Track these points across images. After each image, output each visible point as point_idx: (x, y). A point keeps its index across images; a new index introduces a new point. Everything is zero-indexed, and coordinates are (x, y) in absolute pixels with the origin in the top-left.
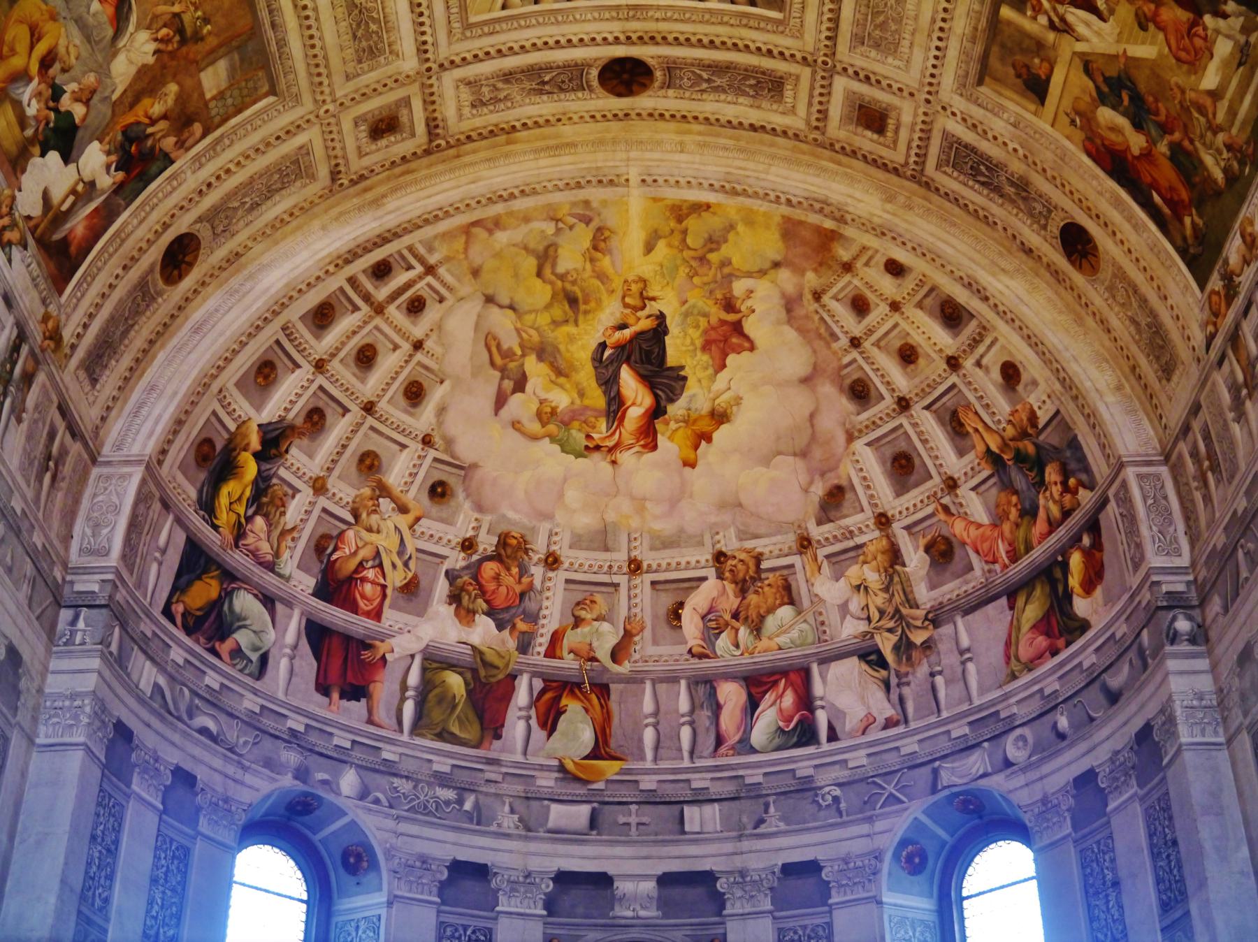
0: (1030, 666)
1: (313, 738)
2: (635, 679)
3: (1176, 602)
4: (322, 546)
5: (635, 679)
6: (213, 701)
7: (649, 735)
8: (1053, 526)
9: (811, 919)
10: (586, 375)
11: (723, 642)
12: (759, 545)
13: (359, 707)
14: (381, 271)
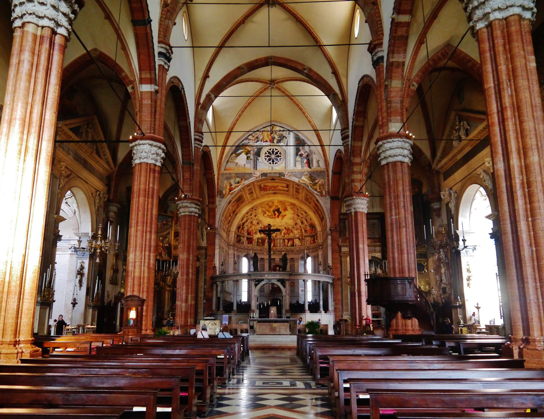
0: (312, 244)
2: (277, 239)
3: (320, 245)
4: (247, 231)
5: (277, 239)
6: (240, 248)
8: (315, 232)
9: (292, 263)
10: (272, 212)
11: (286, 236)
14: (253, 208)
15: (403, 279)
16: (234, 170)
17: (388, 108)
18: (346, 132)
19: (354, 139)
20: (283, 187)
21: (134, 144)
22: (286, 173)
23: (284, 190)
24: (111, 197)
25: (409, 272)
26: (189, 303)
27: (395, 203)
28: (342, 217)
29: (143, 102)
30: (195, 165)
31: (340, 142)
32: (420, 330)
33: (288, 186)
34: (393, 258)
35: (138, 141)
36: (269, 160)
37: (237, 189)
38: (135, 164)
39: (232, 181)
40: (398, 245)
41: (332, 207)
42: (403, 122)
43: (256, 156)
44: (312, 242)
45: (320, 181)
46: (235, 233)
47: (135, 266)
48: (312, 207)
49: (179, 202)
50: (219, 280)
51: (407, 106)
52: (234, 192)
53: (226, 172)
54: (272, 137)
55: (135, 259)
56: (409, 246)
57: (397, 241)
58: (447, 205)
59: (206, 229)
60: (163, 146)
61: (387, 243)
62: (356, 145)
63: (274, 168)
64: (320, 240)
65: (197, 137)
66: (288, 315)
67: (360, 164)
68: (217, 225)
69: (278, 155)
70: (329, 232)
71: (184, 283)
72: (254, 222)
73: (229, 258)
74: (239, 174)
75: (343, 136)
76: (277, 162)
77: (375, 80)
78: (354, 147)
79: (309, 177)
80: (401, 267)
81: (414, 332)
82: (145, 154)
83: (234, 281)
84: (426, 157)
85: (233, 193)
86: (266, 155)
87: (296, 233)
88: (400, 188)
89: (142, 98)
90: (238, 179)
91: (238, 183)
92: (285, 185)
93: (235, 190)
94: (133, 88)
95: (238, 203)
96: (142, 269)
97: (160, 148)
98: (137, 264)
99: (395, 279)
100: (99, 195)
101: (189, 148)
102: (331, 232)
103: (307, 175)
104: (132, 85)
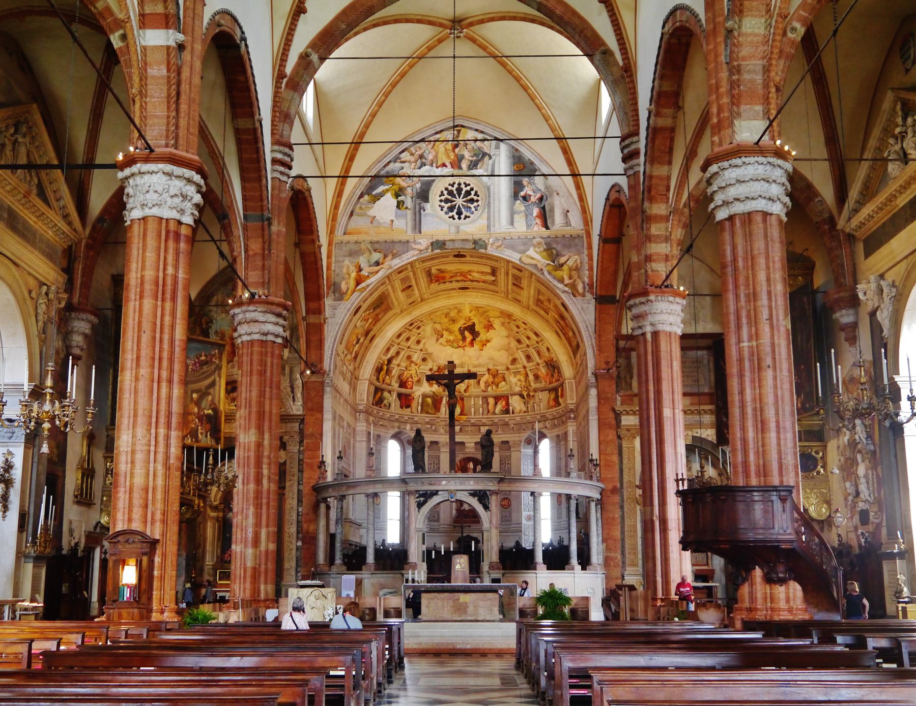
0: (552, 407)
1: (401, 420)
2: (470, 397)
3: (572, 411)
4: (399, 377)
5: (470, 397)
6: (382, 418)
7: (473, 410)
9: (507, 454)
10: (457, 333)
11: (489, 389)
12: (498, 368)
13: (409, 410)
15: (766, 489)
16: (366, 233)
17: (734, 85)
18: (632, 143)
19: (652, 159)
20: (482, 273)
21: (127, 172)
22: (491, 241)
23: (484, 282)
24: (76, 300)
25: (781, 474)
26: (263, 547)
27: (749, 311)
28: (622, 344)
29: (149, 71)
30: (275, 222)
31: (620, 167)
32: (806, 610)
33: (494, 272)
34: (745, 441)
35: (139, 165)
36: (451, 209)
37: (373, 280)
38: (132, 220)
39: (363, 261)
40: (755, 409)
41: (599, 319)
42: (769, 119)
43: (418, 201)
44: (552, 403)
45: (571, 259)
46: (371, 383)
47: (133, 462)
48: (551, 321)
49: (237, 310)
50: (333, 494)
51: (778, 79)
52: (368, 286)
53: (347, 238)
54: (456, 155)
55: (134, 444)
56: (781, 412)
57: (754, 400)
58: (873, 314)
59: (302, 373)
60: (197, 178)
61: (730, 405)
62: (655, 173)
63: (462, 228)
64: (570, 399)
65: (279, 156)
66: (497, 575)
67: (666, 219)
68: (327, 364)
69: (471, 197)
70: (593, 380)
71: (251, 501)
72: (416, 357)
73: (355, 440)
74: (378, 242)
75: (626, 151)
76: (468, 214)
77: (702, 16)
78: (651, 177)
79: (545, 250)
80: (761, 462)
81: (792, 614)
82: (156, 196)
83: (367, 496)
84: (823, 202)
85: (365, 288)
86: (443, 198)
87: (515, 382)
88: (762, 276)
89: (146, 64)
90: (376, 256)
91: (377, 263)
92: (489, 270)
93: (368, 281)
94: (124, 37)
95: (378, 311)
96: (151, 469)
97: (189, 181)
98: (139, 456)
99: (747, 489)
100: (47, 294)
101: (260, 181)
102: (597, 380)
103: (539, 244)
104: (121, 32)
